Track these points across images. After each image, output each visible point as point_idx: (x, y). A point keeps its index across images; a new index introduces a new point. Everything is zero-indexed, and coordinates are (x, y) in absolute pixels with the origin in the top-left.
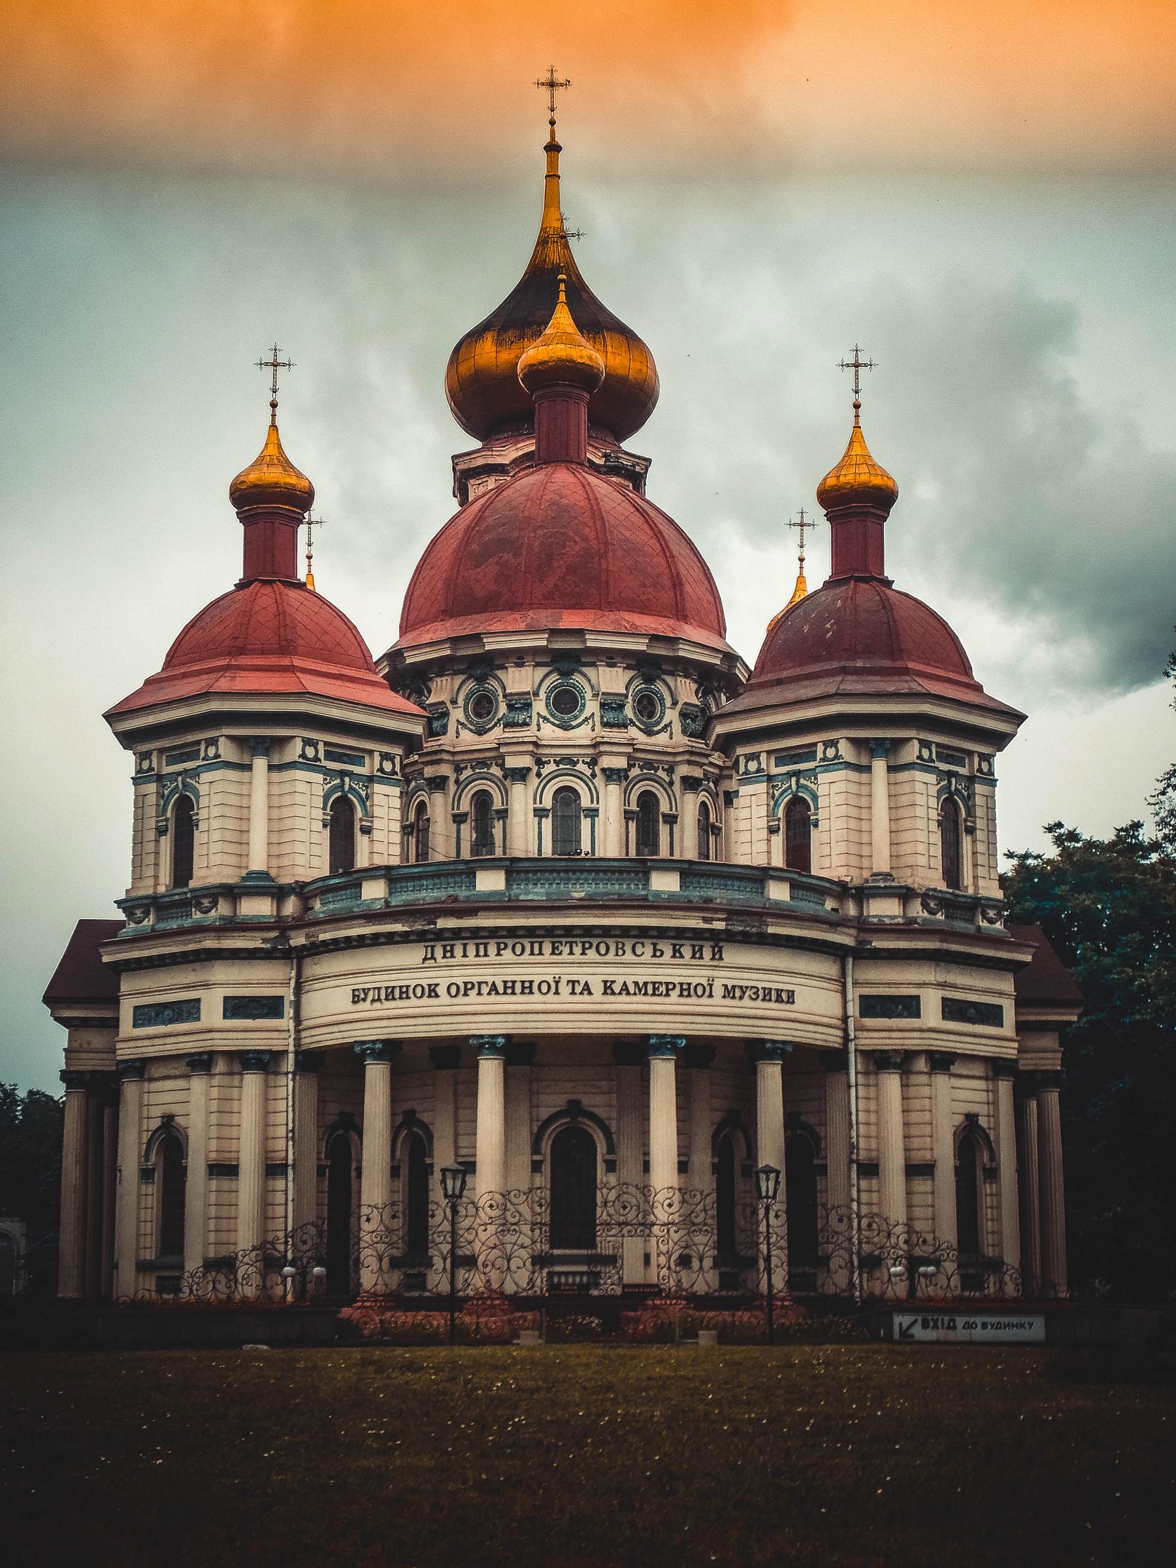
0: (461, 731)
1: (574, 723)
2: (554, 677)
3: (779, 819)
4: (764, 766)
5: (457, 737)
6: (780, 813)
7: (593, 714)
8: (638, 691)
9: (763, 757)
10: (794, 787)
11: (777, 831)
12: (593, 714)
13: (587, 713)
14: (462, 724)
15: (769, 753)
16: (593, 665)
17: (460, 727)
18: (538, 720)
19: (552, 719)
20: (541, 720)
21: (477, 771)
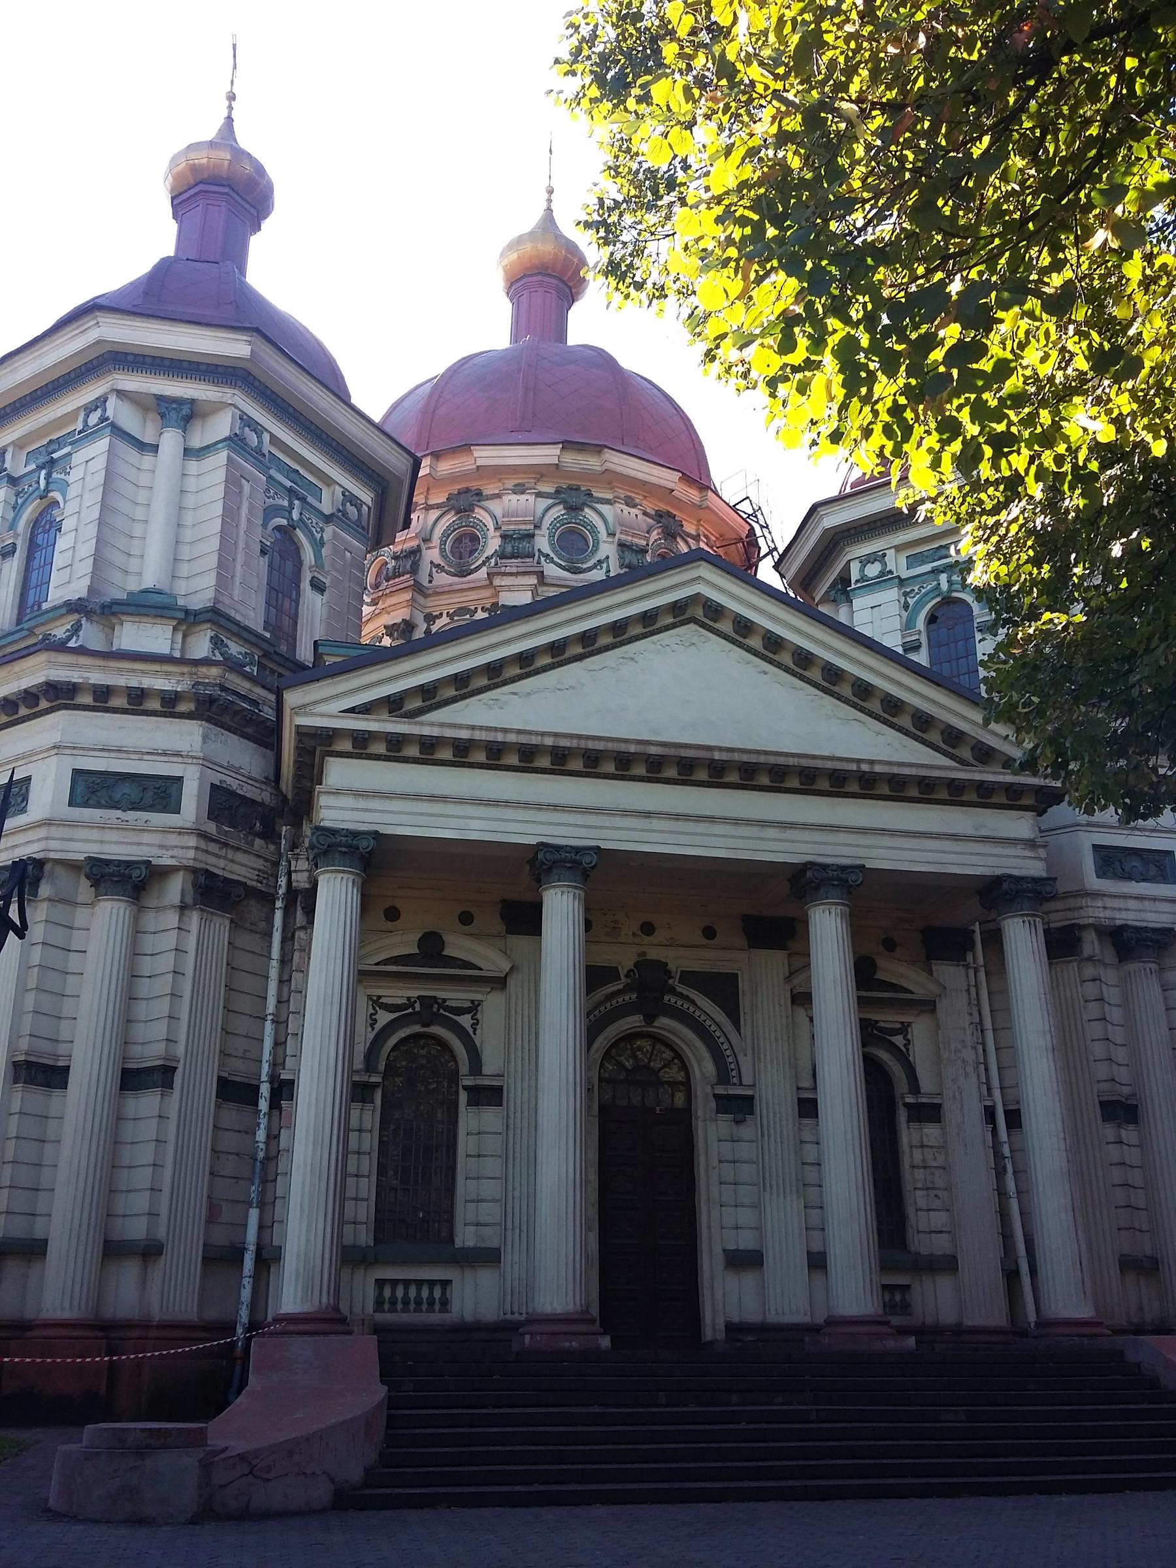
0: (435, 574)
1: (585, 566)
2: (558, 511)
3: (920, 632)
4: (891, 566)
5: (430, 582)
6: (920, 623)
7: (607, 557)
8: (659, 545)
9: (891, 553)
10: (944, 586)
11: (919, 647)
12: (607, 557)
13: (601, 555)
14: (438, 566)
15: (898, 548)
16: (608, 502)
17: (434, 570)
18: (539, 557)
19: (556, 559)
20: (543, 559)
21: (456, 618)
